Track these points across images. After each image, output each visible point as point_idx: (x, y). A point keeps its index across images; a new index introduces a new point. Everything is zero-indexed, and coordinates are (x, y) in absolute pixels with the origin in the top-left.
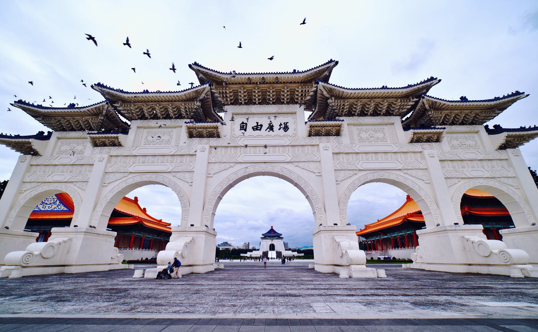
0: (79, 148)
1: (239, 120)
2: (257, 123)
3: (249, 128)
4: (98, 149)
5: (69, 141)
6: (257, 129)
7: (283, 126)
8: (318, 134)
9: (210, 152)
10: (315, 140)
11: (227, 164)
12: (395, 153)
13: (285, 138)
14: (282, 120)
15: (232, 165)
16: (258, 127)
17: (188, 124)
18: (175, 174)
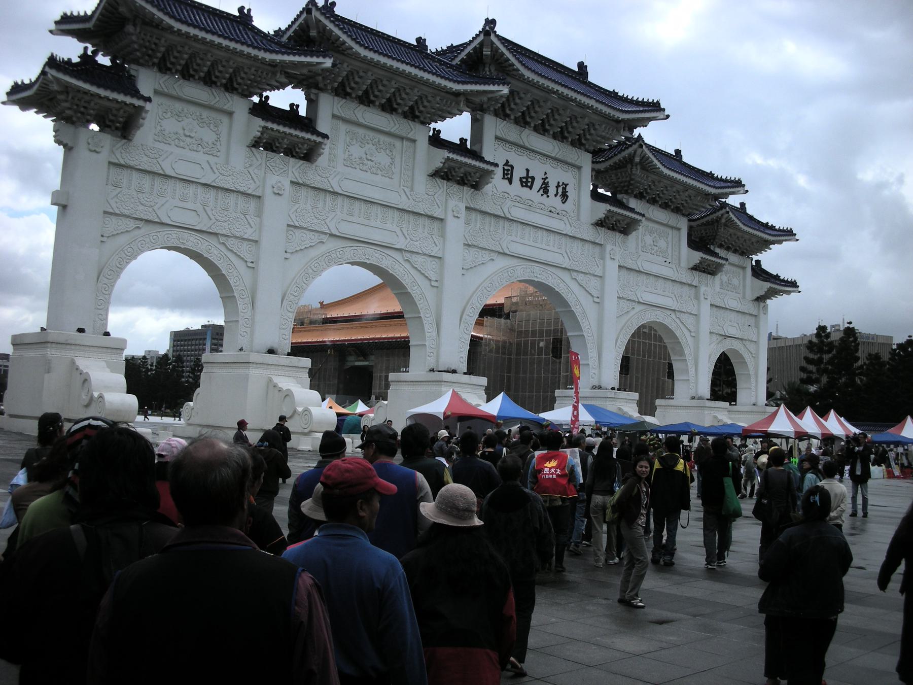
0: (208, 135)
2: (528, 171)
3: (516, 180)
5: (178, 106)
6: (527, 186)
7: (560, 190)
10: (602, 235)
11: (487, 253)
15: (494, 256)
16: (527, 182)
18: (408, 255)
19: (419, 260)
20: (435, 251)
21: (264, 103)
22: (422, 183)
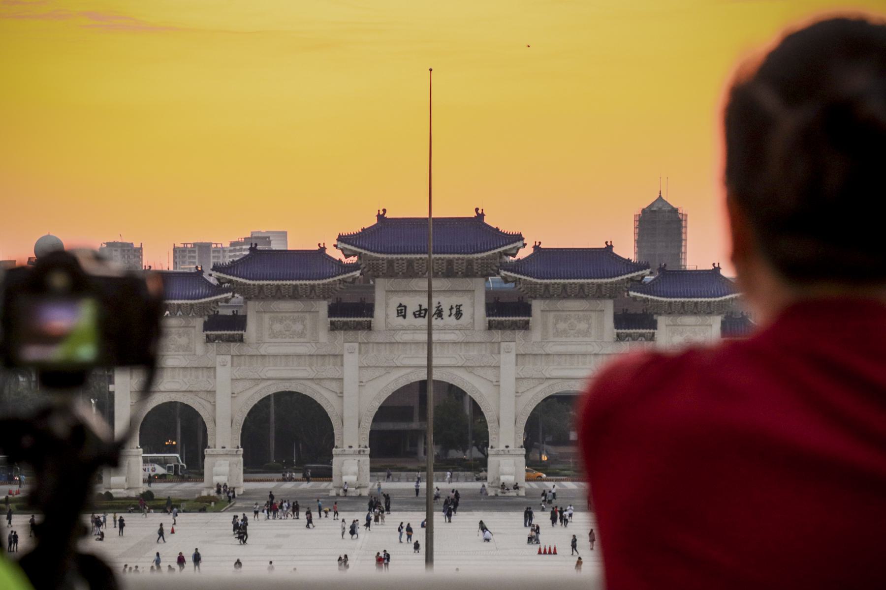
1: (395, 301)
2: (420, 306)
4: (213, 347)
6: (420, 316)
7: (454, 311)
8: (500, 326)
9: (360, 353)
10: (497, 335)
12: (595, 354)
13: (457, 332)
14: (455, 300)
17: (333, 319)
19: (327, 384)
20: (337, 375)
21: (217, 315)
22: (324, 336)
